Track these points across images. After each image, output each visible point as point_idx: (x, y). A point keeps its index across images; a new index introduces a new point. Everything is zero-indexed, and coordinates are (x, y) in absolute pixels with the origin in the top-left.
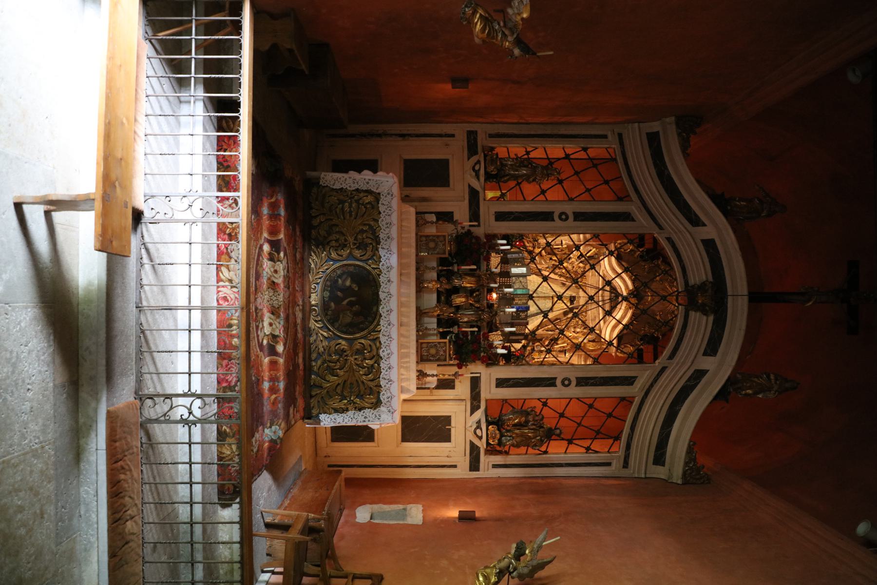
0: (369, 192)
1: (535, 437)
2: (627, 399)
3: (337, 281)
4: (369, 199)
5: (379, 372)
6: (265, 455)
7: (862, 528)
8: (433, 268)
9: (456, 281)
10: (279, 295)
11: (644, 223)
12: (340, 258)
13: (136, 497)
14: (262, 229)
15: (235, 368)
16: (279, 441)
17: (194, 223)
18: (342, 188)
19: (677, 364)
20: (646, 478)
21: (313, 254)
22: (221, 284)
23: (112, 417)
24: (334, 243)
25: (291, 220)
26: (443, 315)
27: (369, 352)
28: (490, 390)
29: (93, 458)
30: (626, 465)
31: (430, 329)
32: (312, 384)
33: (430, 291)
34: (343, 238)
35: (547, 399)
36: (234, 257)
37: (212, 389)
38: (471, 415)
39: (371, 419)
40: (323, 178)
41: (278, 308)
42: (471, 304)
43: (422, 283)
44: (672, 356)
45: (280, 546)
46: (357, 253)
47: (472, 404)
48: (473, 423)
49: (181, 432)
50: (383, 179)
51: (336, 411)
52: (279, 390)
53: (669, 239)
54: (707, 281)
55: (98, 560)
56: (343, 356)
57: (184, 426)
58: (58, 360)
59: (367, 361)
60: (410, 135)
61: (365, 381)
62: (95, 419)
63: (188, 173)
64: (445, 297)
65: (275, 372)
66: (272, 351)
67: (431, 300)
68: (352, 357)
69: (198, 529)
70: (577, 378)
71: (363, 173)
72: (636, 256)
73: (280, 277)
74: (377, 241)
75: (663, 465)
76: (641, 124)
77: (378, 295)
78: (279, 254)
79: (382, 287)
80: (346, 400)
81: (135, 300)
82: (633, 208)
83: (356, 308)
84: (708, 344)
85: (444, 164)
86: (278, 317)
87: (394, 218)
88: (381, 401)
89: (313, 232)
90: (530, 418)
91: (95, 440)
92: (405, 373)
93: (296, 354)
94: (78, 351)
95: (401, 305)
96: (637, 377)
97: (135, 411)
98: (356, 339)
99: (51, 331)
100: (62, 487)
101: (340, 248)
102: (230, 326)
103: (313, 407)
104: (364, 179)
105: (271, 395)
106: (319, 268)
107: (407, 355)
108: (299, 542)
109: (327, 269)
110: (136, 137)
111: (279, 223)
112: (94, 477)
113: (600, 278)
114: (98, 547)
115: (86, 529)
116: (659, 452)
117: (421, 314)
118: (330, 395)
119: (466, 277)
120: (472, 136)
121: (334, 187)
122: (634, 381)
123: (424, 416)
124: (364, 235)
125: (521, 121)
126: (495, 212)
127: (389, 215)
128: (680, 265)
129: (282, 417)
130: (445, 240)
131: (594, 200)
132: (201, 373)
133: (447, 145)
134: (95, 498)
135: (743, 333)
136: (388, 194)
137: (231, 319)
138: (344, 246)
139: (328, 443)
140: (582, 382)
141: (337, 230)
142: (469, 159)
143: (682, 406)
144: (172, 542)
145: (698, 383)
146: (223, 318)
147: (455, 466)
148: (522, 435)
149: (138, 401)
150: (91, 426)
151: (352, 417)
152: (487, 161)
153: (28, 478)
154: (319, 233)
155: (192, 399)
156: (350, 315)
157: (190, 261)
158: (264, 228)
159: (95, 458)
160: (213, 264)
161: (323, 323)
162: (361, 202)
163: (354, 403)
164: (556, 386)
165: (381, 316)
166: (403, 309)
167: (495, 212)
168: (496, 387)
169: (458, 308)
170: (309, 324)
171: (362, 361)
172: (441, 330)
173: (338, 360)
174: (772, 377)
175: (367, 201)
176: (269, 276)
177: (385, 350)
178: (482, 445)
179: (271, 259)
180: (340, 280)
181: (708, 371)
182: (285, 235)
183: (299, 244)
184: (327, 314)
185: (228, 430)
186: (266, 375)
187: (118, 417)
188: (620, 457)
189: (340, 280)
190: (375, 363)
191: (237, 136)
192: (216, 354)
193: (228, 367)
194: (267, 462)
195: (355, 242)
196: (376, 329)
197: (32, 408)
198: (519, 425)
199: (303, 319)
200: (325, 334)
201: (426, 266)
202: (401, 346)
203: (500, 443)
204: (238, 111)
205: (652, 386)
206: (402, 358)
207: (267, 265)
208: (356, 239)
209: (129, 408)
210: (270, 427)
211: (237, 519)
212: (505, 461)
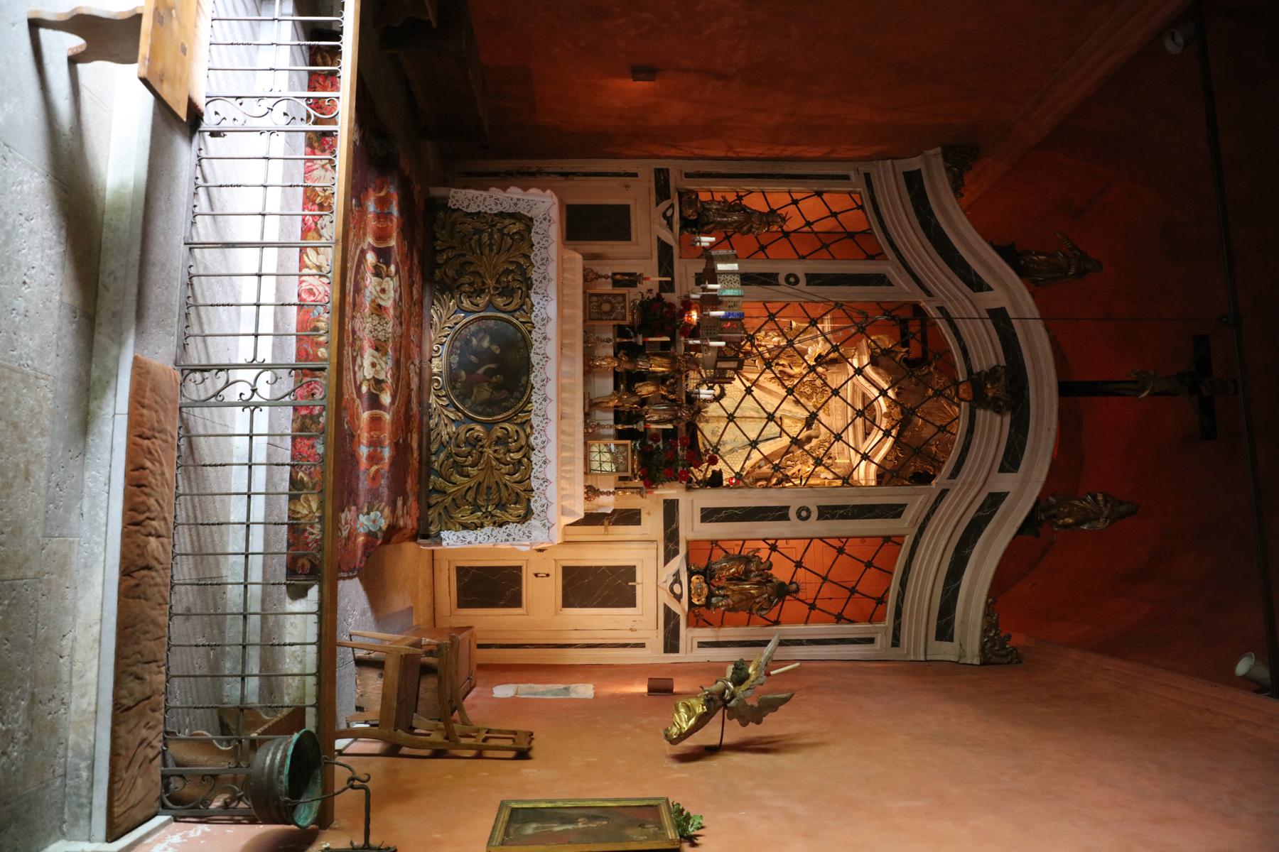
0: (516, 216)
1: (760, 596)
2: (892, 539)
3: (470, 341)
4: (516, 228)
5: (529, 467)
6: (359, 554)
7: (1242, 667)
8: (608, 341)
9: (640, 363)
10: (386, 323)
11: (904, 286)
12: (474, 308)
13: (166, 508)
14: (365, 229)
15: (321, 389)
16: (380, 535)
17: (256, 407)
18: (480, 212)
19: (963, 484)
20: (926, 661)
21: (435, 302)
22: (305, 271)
23: (140, 367)
24: (466, 288)
25: (407, 230)
26: (623, 406)
27: (515, 441)
28: (691, 528)
29: (107, 429)
30: (896, 642)
31: (603, 427)
32: (431, 488)
33: (602, 372)
34: (479, 281)
35: (776, 540)
36: (325, 234)
37: (291, 358)
38: (665, 564)
39: (517, 538)
40: (453, 197)
41: (385, 341)
42: (663, 396)
43: (593, 360)
44: (954, 474)
45: (374, 684)
46: (500, 301)
47: (666, 547)
48: (667, 576)
49: (239, 420)
50: (537, 199)
51: (465, 527)
52: (382, 459)
53: (941, 309)
54: (998, 365)
55: (104, 581)
56: (477, 447)
57: (243, 410)
58: (69, 270)
59: (512, 455)
60: (575, 174)
61: (508, 483)
62: (115, 372)
63: (258, 212)
64: (627, 380)
65: (378, 433)
66: (374, 402)
67: (605, 386)
68: (490, 448)
69: (254, 621)
70: (819, 507)
71: (509, 190)
72: (897, 359)
73: (389, 298)
74: (528, 285)
75: (951, 640)
76: (895, 161)
77: (529, 358)
78: (388, 266)
79: (534, 347)
80: (481, 511)
81: (183, 235)
82: (889, 268)
83: (498, 378)
84: (1005, 456)
85: (624, 211)
86: (385, 354)
87: (552, 270)
88: (532, 510)
89: (437, 271)
90: (753, 566)
91: (112, 403)
92: (568, 487)
93: (408, 431)
94: (98, 276)
95: (561, 389)
96: (905, 505)
97: (174, 384)
98: (496, 423)
99: (64, 224)
100: (60, 454)
101: (475, 295)
102: (316, 329)
103: (432, 522)
104: (511, 198)
105: (371, 466)
106: (445, 322)
107: (570, 461)
108: (406, 655)
109: (456, 324)
110: (200, 11)
111: (389, 224)
112: (107, 456)
113: (849, 407)
114: (105, 561)
115: (88, 534)
116: (944, 621)
117: (591, 406)
118: (456, 505)
119: (656, 358)
120: (662, 179)
121: (469, 211)
122: (902, 511)
123: (596, 567)
124: (510, 278)
125: (731, 154)
126: (696, 274)
127: (545, 248)
128: (959, 344)
129: (385, 499)
130: (625, 301)
131: (834, 258)
132: (263, 584)
133: (626, 187)
134: (107, 487)
135: (1053, 434)
136: (545, 219)
137: (318, 321)
138: (480, 292)
139: (453, 608)
140: (827, 513)
141: (472, 269)
142: (657, 204)
143: (973, 548)
144: (216, 616)
145: (995, 511)
146: (306, 317)
147: (642, 645)
148: (742, 592)
149: (178, 374)
150: (108, 382)
151: (489, 534)
152: (684, 203)
153: (12, 407)
154: (445, 273)
155: (259, 371)
156: (487, 388)
157: (251, 430)
158: (369, 230)
159: (111, 428)
160: (297, 186)
161: (449, 399)
162: (506, 231)
163: (493, 516)
164: (789, 520)
165: (533, 387)
166: (565, 395)
167: (696, 274)
168: (702, 522)
169: (644, 402)
170: (429, 399)
171: (505, 454)
172: (620, 427)
173: (470, 454)
174: (1100, 498)
175: (515, 231)
176: (373, 297)
177: (539, 436)
178: (681, 609)
179: (378, 273)
180: (474, 339)
181: (1007, 493)
182: (397, 243)
183: (417, 278)
184: (453, 388)
185: (305, 479)
186: (364, 436)
187: (148, 372)
188: (886, 628)
189: (474, 339)
190: (524, 456)
191: (337, 72)
192: (286, 526)
193: (311, 387)
194: (362, 565)
195: (498, 286)
196: (526, 409)
197: (27, 311)
198: (734, 579)
199: (420, 388)
200: (452, 416)
201: (598, 338)
202: (561, 447)
203: (708, 605)
204: (339, 39)
205: (928, 518)
206: (562, 464)
207: (371, 282)
208: (498, 281)
209: (166, 373)
210: (368, 513)
211: (314, 639)
212: (717, 637)
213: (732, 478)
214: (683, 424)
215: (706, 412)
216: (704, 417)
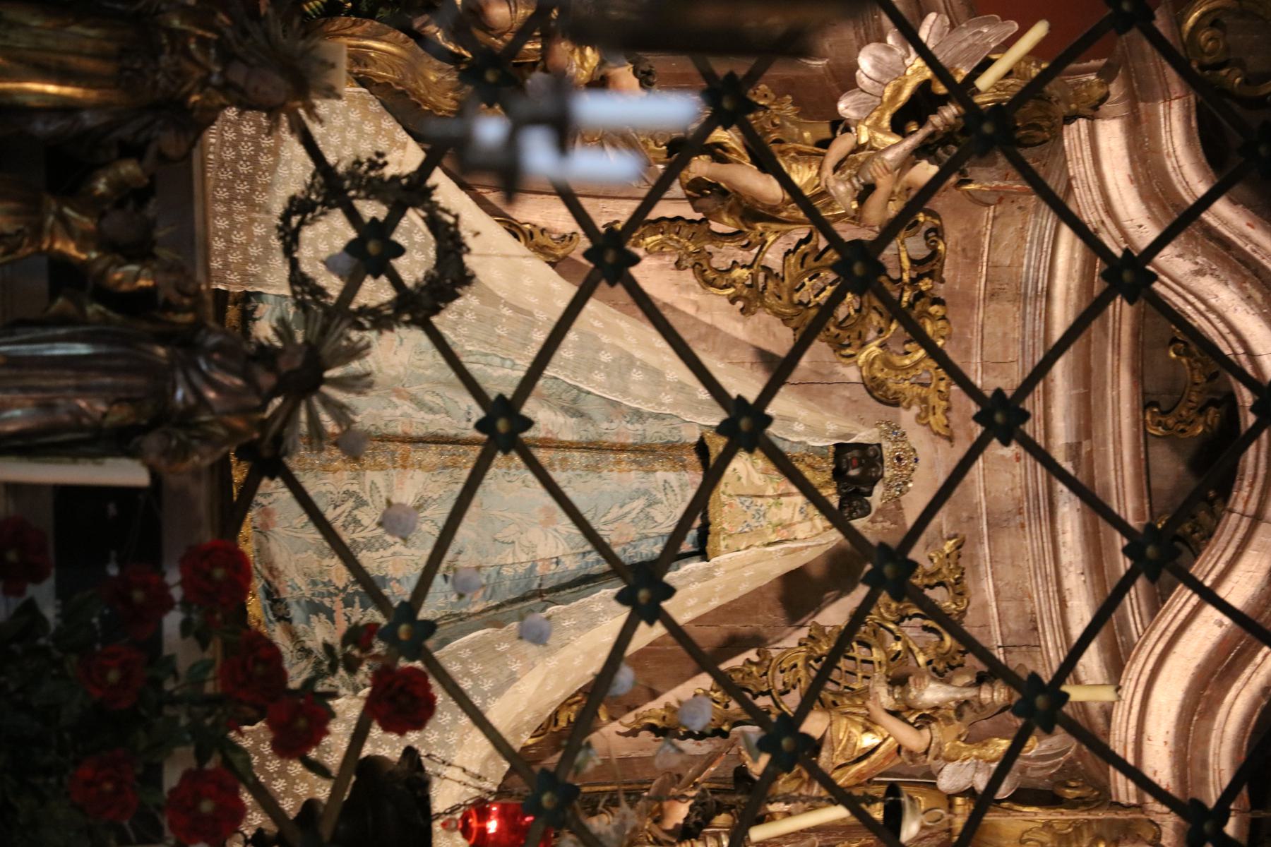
213: (480, 808)
214: (201, 459)
215: (360, 383)
216: (340, 412)
